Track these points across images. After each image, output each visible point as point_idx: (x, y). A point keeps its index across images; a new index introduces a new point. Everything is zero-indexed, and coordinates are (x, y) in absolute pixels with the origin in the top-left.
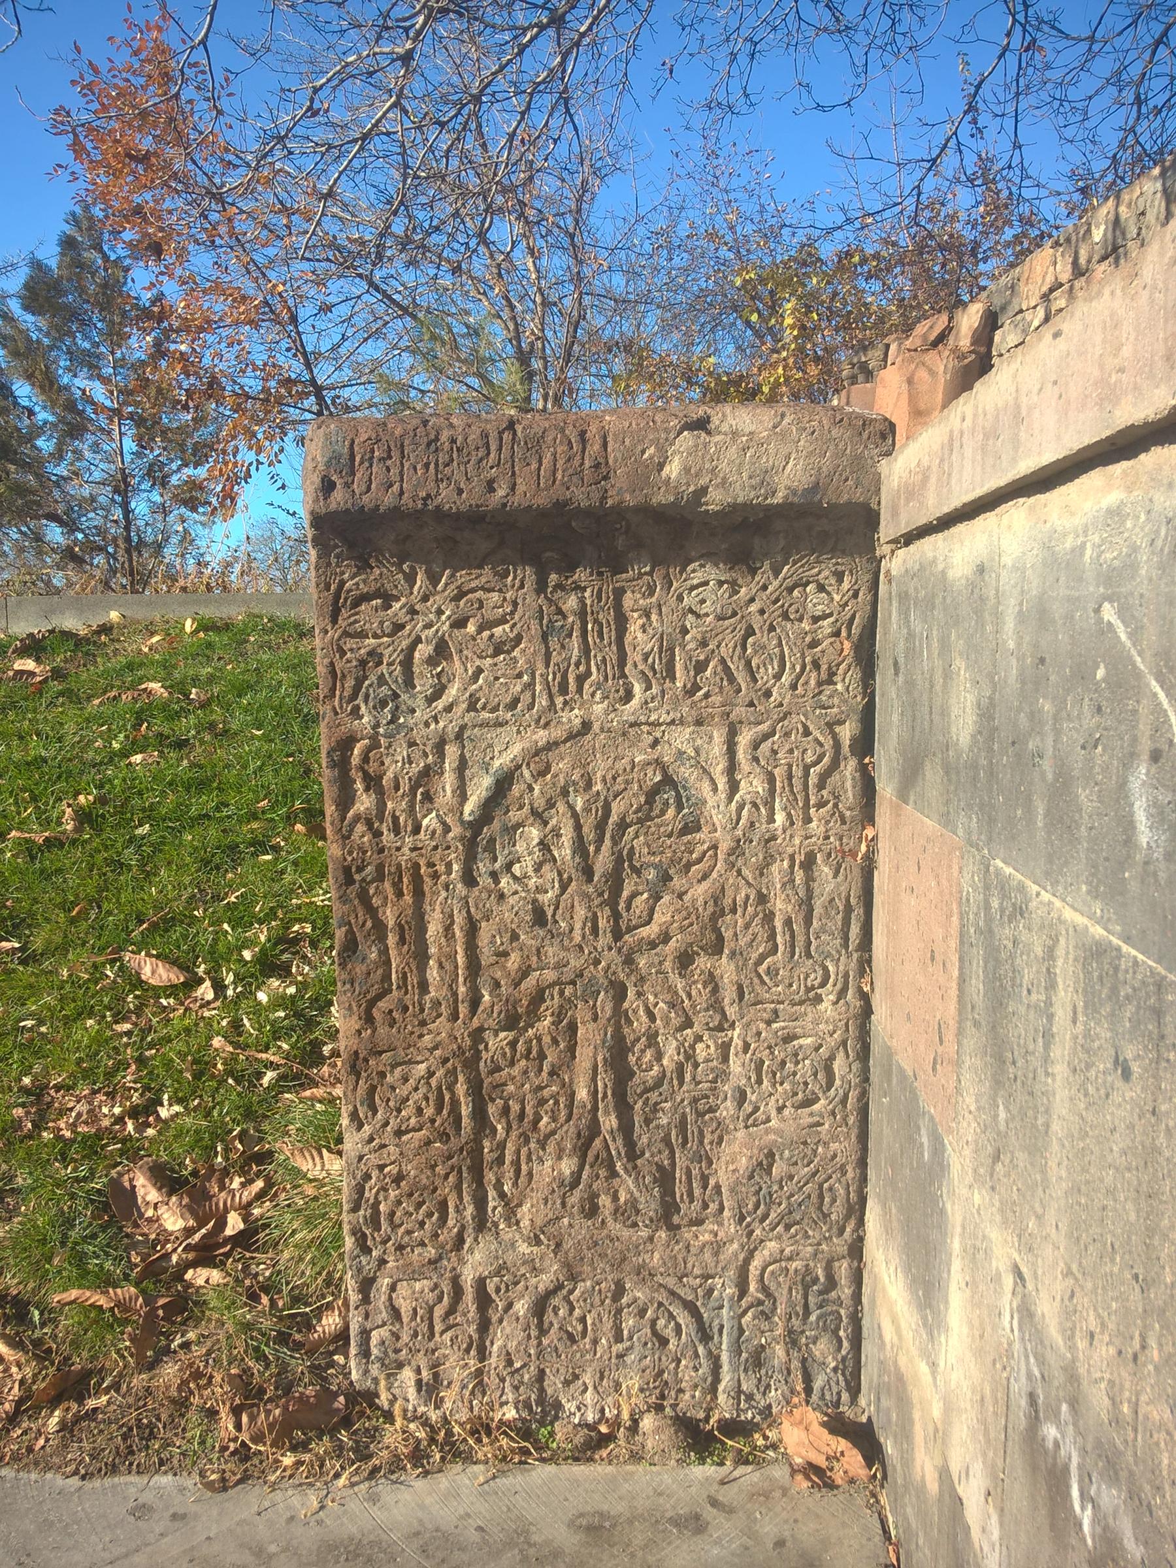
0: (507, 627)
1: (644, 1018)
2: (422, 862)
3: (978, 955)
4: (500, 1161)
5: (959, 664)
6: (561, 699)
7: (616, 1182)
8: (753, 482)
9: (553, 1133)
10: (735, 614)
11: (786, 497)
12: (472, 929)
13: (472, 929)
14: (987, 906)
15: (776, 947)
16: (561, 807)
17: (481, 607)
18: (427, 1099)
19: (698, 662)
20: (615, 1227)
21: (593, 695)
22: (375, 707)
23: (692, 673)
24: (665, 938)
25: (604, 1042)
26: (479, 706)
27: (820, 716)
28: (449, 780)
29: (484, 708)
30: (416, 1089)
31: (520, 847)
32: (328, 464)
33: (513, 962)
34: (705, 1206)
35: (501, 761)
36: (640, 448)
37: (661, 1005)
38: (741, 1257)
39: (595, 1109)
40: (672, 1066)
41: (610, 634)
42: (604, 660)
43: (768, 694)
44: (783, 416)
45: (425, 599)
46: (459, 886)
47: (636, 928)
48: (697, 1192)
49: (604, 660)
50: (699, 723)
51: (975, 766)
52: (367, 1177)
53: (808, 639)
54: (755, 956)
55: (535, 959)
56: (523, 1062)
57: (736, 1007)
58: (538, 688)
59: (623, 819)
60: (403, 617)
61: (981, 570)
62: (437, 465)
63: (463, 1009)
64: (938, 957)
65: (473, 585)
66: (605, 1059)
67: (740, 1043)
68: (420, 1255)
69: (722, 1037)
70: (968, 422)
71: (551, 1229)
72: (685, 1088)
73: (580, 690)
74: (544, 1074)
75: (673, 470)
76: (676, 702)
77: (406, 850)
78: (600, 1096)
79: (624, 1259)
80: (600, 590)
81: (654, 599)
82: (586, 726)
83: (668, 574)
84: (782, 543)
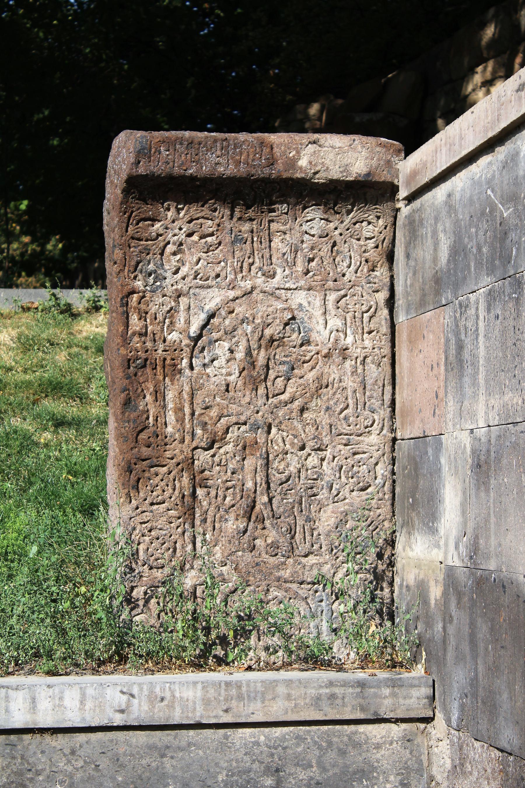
0: (214, 238)
1: (281, 444)
2: (168, 358)
3: (453, 341)
4: (205, 521)
5: (441, 236)
6: (241, 275)
7: (266, 532)
8: (341, 169)
9: (233, 506)
10: (327, 235)
11: (356, 177)
12: (192, 396)
13: (192, 396)
14: (455, 317)
15: (348, 406)
16: (239, 331)
17: (201, 227)
18: (168, 485)
19: (309, 258)
20: (265, 557)
21: (257, 273)
22: (145, 276)
23: (307, 264)
24: (292, 400)
25: (261, 455)
26: (199, 277)
27: (370, 287)
28: (182, 317)
29: (201, 279)
30: (162, 480)
31: (218, 351)
32: (139, 152)
33: (214, 413)
34: (313, 546)
35: (210, 306)
36: (288, 151)
37: (290, 436)
38: (332, 572)
39: (255, 491)
40: (296, 471)
41: (265, 244)
42: (263, 257)
43: (344, 275)
44: (354, 140)
45: (173, 222)
46: (187, 371)
47: (277, 395)
48: (308, 538)
49: (263, 257)
50: (309, 290)
51: (449, 270)
52: (134, 529)
53: (363, 249)
54: (338, 410)
55: (225, 411)
56: (218, 468)
57: (329, 437)
58: (229, 269)
59: (271, 337)
60: (161, 231)
61: (449, 195)
62: (191, 154)
63: (188, 438)
64: (435, 366)
65: (198, 215)
66: (262, 464)
67: (331, 457)
68: (162, 573)
69: (322, 454)
70: (443, 141)
71: (233, 558)
72: (302, 482)
73: (250, 270)
74: (229, 473)
75: (303, 162)
76: (297, 279)
77: (160, 351)
78: (258, 485)
79: (271, 573)
80: (261, 220)
81: (288, 227)
82: (253, 288)
83: (295, 214)
84: (352, 200)
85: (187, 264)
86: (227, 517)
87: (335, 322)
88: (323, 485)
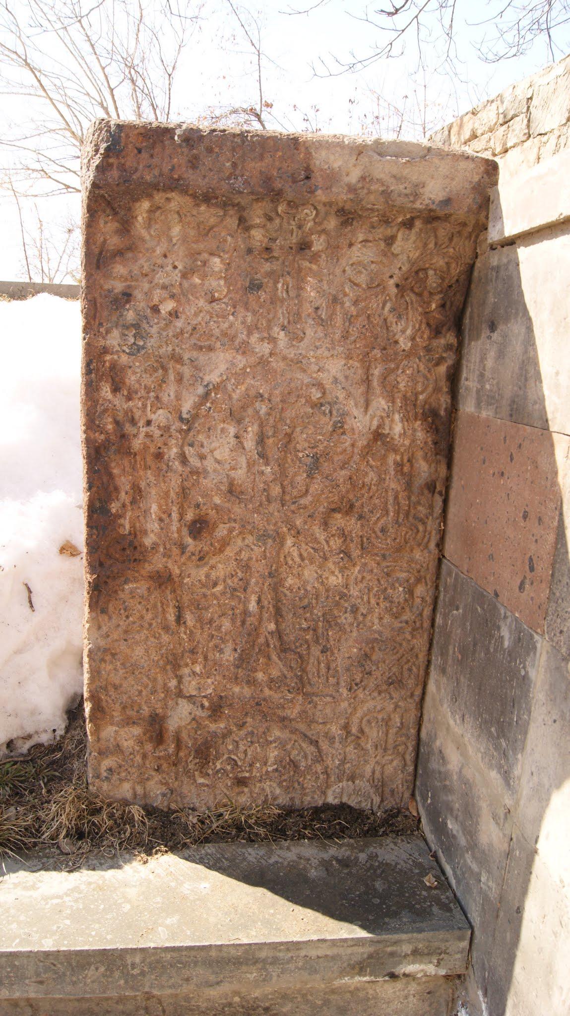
8: (407, 191)
85: (183, 317)
86: (223, 646)
87: (380, 403)
88: (346, 608)
